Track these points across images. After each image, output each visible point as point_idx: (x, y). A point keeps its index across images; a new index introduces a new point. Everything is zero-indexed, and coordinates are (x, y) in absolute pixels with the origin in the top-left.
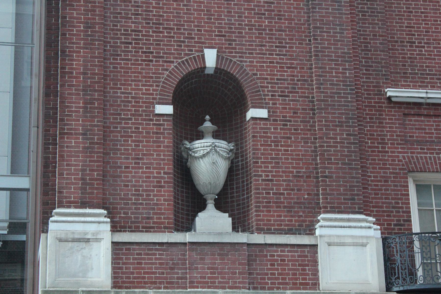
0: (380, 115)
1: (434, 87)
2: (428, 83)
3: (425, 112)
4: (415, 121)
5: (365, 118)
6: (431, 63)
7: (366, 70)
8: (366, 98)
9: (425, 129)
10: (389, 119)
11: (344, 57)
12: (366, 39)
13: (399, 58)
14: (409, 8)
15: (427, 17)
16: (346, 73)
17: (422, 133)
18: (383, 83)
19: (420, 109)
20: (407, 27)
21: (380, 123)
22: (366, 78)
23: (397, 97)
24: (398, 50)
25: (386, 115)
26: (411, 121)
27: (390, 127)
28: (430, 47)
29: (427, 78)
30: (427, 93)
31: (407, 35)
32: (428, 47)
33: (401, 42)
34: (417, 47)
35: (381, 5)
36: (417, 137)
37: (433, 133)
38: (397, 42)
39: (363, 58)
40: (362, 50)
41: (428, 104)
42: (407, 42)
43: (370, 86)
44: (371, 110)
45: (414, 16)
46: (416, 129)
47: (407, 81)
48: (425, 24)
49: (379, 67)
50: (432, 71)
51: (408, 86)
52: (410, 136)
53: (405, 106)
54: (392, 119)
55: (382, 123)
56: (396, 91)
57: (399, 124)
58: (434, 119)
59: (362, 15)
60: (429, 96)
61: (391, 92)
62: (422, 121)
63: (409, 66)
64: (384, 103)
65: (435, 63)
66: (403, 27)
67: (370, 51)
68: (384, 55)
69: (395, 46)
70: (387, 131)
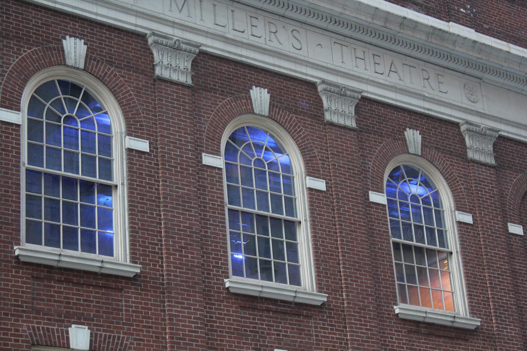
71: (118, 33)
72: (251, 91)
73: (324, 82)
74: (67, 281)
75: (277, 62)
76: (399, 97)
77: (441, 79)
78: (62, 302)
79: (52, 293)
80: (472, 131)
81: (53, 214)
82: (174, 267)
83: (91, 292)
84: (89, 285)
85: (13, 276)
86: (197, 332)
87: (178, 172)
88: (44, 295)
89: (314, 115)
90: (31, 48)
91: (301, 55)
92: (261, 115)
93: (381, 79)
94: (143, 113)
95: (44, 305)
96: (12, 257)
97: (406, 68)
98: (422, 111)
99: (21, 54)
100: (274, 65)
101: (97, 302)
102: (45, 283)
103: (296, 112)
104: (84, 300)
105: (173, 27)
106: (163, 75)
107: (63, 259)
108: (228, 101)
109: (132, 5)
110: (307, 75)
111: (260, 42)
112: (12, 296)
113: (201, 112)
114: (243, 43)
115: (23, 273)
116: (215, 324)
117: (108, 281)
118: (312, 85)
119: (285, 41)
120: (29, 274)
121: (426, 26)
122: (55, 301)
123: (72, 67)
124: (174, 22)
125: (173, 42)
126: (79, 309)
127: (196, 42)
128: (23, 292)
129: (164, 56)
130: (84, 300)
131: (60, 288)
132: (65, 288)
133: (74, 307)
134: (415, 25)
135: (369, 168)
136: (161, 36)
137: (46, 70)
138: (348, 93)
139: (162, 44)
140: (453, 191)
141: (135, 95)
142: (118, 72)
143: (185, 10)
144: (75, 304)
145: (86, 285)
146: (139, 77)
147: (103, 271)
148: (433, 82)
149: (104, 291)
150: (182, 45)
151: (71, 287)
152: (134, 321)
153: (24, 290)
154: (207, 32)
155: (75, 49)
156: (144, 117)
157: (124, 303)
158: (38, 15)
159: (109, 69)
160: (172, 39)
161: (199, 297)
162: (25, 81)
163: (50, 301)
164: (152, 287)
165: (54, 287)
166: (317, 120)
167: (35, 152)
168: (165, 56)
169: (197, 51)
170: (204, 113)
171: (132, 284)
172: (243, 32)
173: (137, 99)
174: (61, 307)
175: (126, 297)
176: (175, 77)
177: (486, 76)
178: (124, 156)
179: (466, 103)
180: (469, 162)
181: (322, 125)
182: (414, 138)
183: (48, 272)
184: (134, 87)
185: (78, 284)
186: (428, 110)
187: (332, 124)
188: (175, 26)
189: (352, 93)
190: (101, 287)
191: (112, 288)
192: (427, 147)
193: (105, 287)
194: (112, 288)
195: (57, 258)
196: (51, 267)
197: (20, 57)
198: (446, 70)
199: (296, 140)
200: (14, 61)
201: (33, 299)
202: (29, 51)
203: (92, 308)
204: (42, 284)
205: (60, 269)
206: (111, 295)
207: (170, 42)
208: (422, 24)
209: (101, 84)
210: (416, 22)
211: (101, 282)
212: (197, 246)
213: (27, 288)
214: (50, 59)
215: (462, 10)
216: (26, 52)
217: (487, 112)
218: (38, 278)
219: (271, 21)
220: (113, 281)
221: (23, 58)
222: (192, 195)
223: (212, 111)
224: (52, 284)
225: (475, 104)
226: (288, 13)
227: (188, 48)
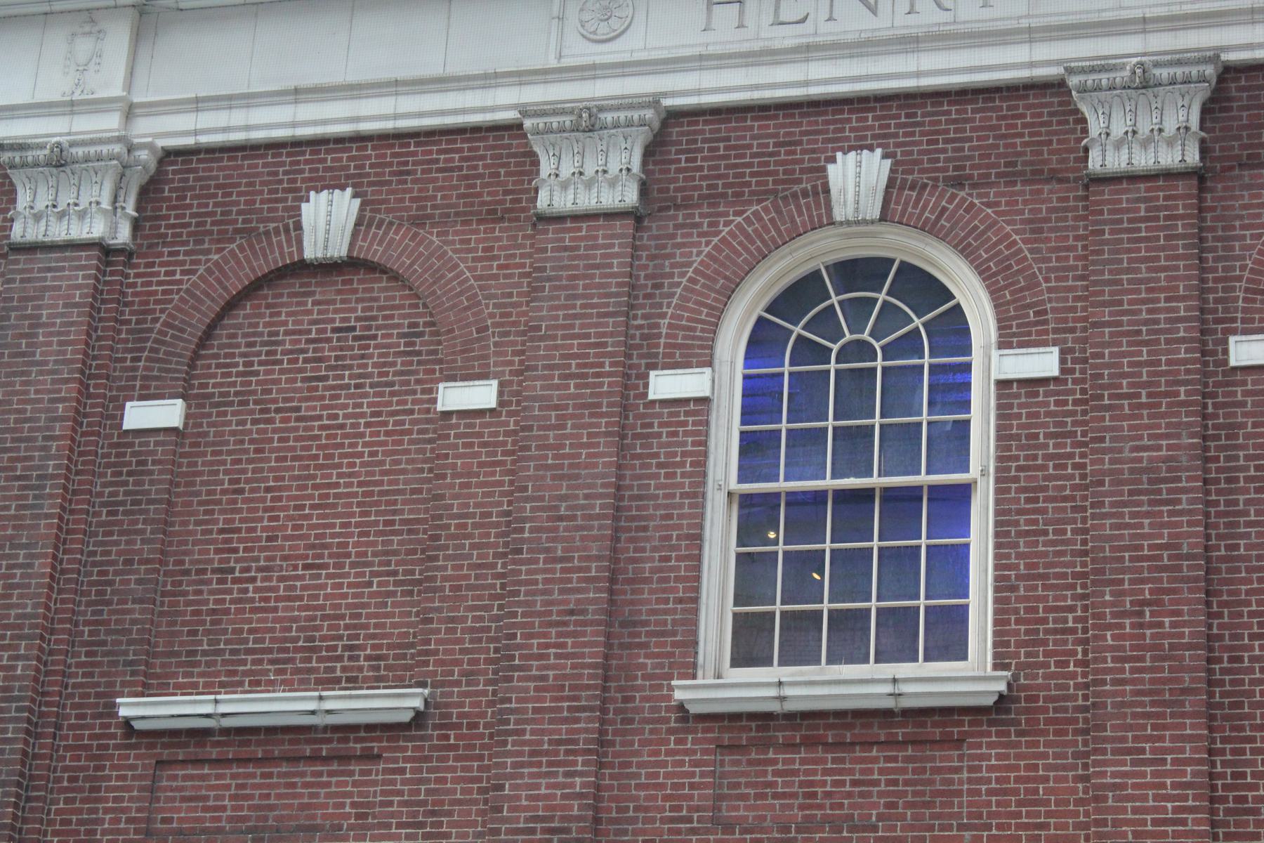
0: (97, 768)
1: (258, 683)
2: (245, 673)
3: (214, 753)
4: (185, 778)
5: (58, 780)
6: (265, 620)
7: (88, 654)
8: (71, 727)
9: (206, 798)
10: (119, 778)
11: (20, 627)
12: (105, 573)
13: (184, 613)
14: (238, 481)
15: (280, 499)
16: (14, 668)
17: (195, 809)
18: (123, 684)
19: (201, 745)
20: (221, 531)
21: (92, 789)
22: (85, 675)
23: (143, 718)
24: (185, 593)
25: (113, 767)
26: (175, 778)
27: (116, 800)
28: (269, 579)
29: (244, 662)
30: (216, 701)
31: (217, 551)
32: (264, 579)
33: (199, 572)
34: (235, 581)
35: (160, 482)
36: (181, 820)
37: (224, 808)
38: (187, 572)
39: (87, 623)
40: (89, 604)
41: (226, 731)
42: (214, 571)
43: (88, 696)
44: (78, 758)
45: (245, 501)
46: (183, 799)
47: (191, 675)
48: (271, 519)
49: (121, 643)
50: (262, 640)
51: (184, 689)
52: (164, 821)
53: (165, 740)
54: (124, 778)
55: (98, 789)
56: (138, 704)
57: (141, 789)
58: (235, 771)
59: (109, 513)
60: (223, 709)
61: (128, 707)
62: (202, 778)
63: (207, 632)
64: (113, 736)
65: (275, 620)
66: (211, 532)
67: (109, 603)
68: (143, 611)
69: (180, 583)
70: (106, 811)
71: (985, 100)
74: (811, 743)
78: (794, 795)
79: (770, 778)
81: (801, 586)
82: (1114, 659)
83: (875, 760)
84: (867, 745)
85: (670, 753)
86: (1183, 822)
87: (1141, 406)
88: (747, 785)
90: (744, 212)
94: (1047, 280)
95: (747, 808)
96: (668, 709)
99: (717, 233)
101: (889, 782)
102: (753, 756)
104: (855, 783)
105: (1144, 31)
106: (1109, 166)
107: (788, 691)
109: (1028, 16)
112: (666, 798)
113: (1234, 228)
115: (694, 742)
116: (1250, 794)
117: (923, 725)
120: (710, 741)
122: (776, 796)
123: (848, 223)
124: (1144, 20)
125: (1127, 73)
126: (841, 806)
127: (1198, 50)
128: (692, 786)
129: (1114, 115)
130: (855, 783)
131: (793, 761)
132: (803, 761)
133: (828, 802)
136: (1093, 70)
137: (785, 249)
139: (1098, 89)
141: (1025, 241)
142: (979, 196)
144: (828, 795)
145: (861, 744)
146: (1040, 192)
147: (906, 703)
149: (910, 752)
150: (1157, 72)
151: (820, 755)
152: (991, 815)
153: (697, 780)
155: (856, 177)
156: (1050, 290)
157: (965, 775)
158: (768, 127)
159: (953, 196)
161: (1193, 726)
162: (728, 294)
163: (763, 796)
164: (1049, 721)
165: (774, 762)
167: (755, 450)
168: (1117, 116)
169: (1210, 70)
170: (1243, 227)
171: (991, 723)
173: (1031, 251)
174: (791, 807)
175: (972, 757)
176: (1144, 160)
183: (758, 729)
184: (1023, 222)
185: (839, 745)
190: (905, 743)
191: (933, 742)
193: (914, 742)
194: (933, 742)
195: (773, 692)
196: (768, 716)
197: (716, 240)
200: (699, 254)
201: (721, 798)
202: (739, 219)
203: (875, 799)
204: (744, 758)
205: (790, 716)
206: (933, 759)
207: (1122, 76)
209: (931, 240)
211: (900, 733)
212: (1190, 590)
213: (703, 775)
214: (793, 221)
216: (732, 222)
218: (733, 748)
220: (935, 725)
221: (723, 240)
222: (1184, 459)
224: (771, 755)
227: (1179, 71)
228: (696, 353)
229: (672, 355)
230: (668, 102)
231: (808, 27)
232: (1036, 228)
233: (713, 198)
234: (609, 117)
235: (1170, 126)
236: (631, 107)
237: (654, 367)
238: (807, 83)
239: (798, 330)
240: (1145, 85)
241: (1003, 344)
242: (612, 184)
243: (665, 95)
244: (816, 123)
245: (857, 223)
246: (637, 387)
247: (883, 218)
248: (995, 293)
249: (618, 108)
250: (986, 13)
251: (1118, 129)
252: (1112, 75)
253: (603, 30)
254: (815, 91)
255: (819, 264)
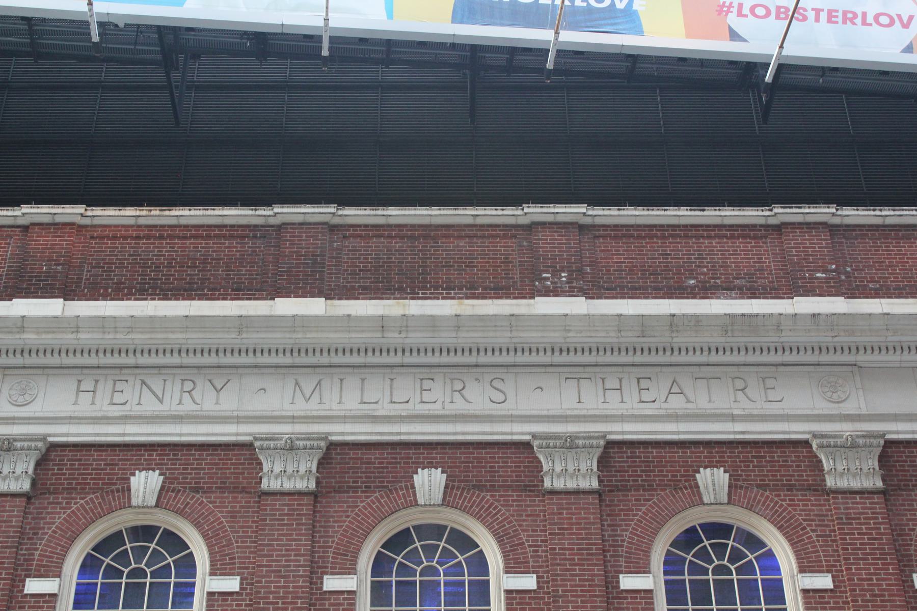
72: (415, 476)
73: (534, 436)
75: (459, 427)
76: (683, 427)
77: (770, 383)
80: (829, 446)
89: (526, 486)
91: (510, 407)
92: (430, 505)
93: (648, 409)
94: (237, 542)
97: (702, 383)
98: (731, 437)
100: (456, 433)
103: (493, 488)
105: (293, 423)
108: (376, 497)
109: (237, 410)
110: (512, 433)
111: (436, 409)
113: (329, 521)
114: (401, 417)
118: (527, 445)
119: (478, 397)
121: (717, 316)
123: (139, 507)
124: (293, 417)
125: (283, 442)
134: (697, 321)
135: (623, 541)
136: (267, 439)
137: (105, 518)
138: (581, 442)
139: (269, 449)
140: (793, 544)
141: (227, 522)
142: (206, 498)
143: (316, 394)
148: (755, 391)
150: (298, 443)
154: (345, 417)
155: (145, 484)
156: (238, 547)
158: (102, 455)
159: (193, 497)
160: (281, 439)
162: (72, 540)
166: (530, 491)
168: (277, 463)
169: (323, 444)
172: (407, 402)
173: (230, 527)
176: (288, 486)
177: (861, 358)
178: (205, 603)
179: (833, 409)
180: (828, 495)
181: (538, 496)
182: (713, 481)
184: (227, 512)
186: (743, 433)
187: (553, 492)
188: (295, 420)
189: (587, 442)
192: (741, 487)
198: (781, 369)
199: (489, 527)
200: (59, 518)
208: (707, 316)
209: (180, 519)
210: (696, 316)
214: (110, 504)
215: (819, 275)
217: (864, 411)
219: (457, 376)
221: (73, 512)
223: (348, 517)
225: (841, 405)
226: (483, 359)
227: (308, 443)
228: (53, 570)
229: (39, 571)
230: (51, 439)
231: (127, 407)
232: (233, 515)
233: (70, 490)
234: (19, 444)
235: (302, 470)
236: (31, 440)
237: (29, 576)
238: (124, 435)
239: (108, 561)
240: (292, 449)
241: (211, 574)
242: (17, 479)
243: (50, 435)
244: (127, 455)
245: (143, 507)
246: (18, 586)
247: (157, 506)
248: (210, 547)
249: (24, 440)
250: (217, 407)
251: (277, 469)
252: (276, 442)
253: (21, 400)
254: (127, 439)
255: (121, 527)
